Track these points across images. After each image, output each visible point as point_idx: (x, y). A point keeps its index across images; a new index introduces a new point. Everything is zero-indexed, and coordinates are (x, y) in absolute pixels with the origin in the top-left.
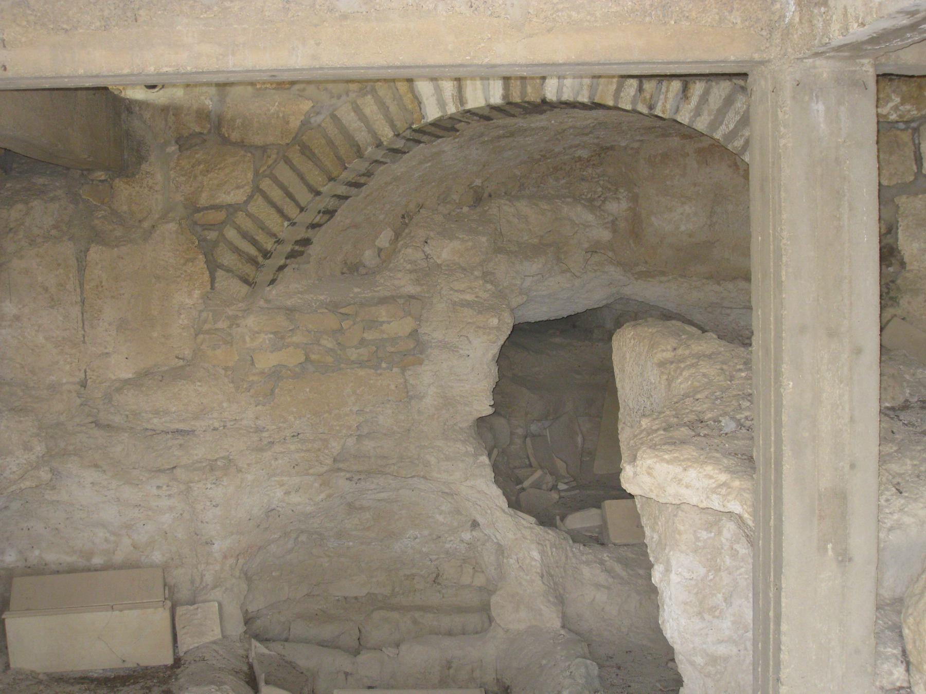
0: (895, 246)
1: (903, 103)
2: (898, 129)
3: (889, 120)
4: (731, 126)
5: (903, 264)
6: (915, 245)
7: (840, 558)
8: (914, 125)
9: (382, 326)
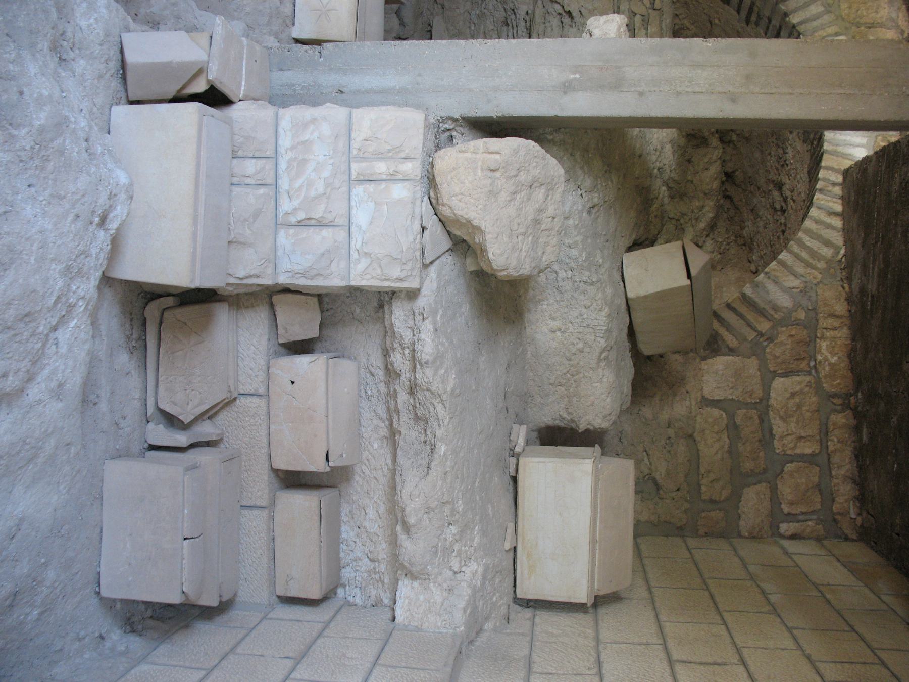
0: (719, 353)
1: (830, 364)
2: (809, 361)
3: (816, 355)
4: (808, 244)
5: (704, 359)
6: (721, 367)
7: (566, 85)
8: (813, 371)
9: (644, 29)
